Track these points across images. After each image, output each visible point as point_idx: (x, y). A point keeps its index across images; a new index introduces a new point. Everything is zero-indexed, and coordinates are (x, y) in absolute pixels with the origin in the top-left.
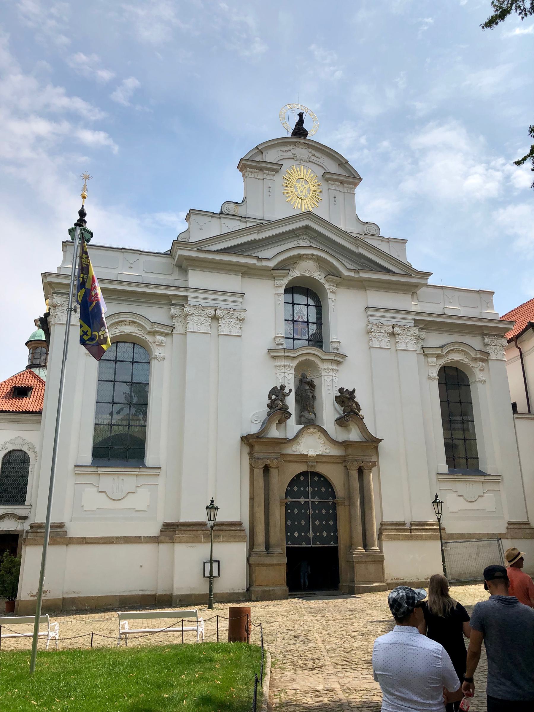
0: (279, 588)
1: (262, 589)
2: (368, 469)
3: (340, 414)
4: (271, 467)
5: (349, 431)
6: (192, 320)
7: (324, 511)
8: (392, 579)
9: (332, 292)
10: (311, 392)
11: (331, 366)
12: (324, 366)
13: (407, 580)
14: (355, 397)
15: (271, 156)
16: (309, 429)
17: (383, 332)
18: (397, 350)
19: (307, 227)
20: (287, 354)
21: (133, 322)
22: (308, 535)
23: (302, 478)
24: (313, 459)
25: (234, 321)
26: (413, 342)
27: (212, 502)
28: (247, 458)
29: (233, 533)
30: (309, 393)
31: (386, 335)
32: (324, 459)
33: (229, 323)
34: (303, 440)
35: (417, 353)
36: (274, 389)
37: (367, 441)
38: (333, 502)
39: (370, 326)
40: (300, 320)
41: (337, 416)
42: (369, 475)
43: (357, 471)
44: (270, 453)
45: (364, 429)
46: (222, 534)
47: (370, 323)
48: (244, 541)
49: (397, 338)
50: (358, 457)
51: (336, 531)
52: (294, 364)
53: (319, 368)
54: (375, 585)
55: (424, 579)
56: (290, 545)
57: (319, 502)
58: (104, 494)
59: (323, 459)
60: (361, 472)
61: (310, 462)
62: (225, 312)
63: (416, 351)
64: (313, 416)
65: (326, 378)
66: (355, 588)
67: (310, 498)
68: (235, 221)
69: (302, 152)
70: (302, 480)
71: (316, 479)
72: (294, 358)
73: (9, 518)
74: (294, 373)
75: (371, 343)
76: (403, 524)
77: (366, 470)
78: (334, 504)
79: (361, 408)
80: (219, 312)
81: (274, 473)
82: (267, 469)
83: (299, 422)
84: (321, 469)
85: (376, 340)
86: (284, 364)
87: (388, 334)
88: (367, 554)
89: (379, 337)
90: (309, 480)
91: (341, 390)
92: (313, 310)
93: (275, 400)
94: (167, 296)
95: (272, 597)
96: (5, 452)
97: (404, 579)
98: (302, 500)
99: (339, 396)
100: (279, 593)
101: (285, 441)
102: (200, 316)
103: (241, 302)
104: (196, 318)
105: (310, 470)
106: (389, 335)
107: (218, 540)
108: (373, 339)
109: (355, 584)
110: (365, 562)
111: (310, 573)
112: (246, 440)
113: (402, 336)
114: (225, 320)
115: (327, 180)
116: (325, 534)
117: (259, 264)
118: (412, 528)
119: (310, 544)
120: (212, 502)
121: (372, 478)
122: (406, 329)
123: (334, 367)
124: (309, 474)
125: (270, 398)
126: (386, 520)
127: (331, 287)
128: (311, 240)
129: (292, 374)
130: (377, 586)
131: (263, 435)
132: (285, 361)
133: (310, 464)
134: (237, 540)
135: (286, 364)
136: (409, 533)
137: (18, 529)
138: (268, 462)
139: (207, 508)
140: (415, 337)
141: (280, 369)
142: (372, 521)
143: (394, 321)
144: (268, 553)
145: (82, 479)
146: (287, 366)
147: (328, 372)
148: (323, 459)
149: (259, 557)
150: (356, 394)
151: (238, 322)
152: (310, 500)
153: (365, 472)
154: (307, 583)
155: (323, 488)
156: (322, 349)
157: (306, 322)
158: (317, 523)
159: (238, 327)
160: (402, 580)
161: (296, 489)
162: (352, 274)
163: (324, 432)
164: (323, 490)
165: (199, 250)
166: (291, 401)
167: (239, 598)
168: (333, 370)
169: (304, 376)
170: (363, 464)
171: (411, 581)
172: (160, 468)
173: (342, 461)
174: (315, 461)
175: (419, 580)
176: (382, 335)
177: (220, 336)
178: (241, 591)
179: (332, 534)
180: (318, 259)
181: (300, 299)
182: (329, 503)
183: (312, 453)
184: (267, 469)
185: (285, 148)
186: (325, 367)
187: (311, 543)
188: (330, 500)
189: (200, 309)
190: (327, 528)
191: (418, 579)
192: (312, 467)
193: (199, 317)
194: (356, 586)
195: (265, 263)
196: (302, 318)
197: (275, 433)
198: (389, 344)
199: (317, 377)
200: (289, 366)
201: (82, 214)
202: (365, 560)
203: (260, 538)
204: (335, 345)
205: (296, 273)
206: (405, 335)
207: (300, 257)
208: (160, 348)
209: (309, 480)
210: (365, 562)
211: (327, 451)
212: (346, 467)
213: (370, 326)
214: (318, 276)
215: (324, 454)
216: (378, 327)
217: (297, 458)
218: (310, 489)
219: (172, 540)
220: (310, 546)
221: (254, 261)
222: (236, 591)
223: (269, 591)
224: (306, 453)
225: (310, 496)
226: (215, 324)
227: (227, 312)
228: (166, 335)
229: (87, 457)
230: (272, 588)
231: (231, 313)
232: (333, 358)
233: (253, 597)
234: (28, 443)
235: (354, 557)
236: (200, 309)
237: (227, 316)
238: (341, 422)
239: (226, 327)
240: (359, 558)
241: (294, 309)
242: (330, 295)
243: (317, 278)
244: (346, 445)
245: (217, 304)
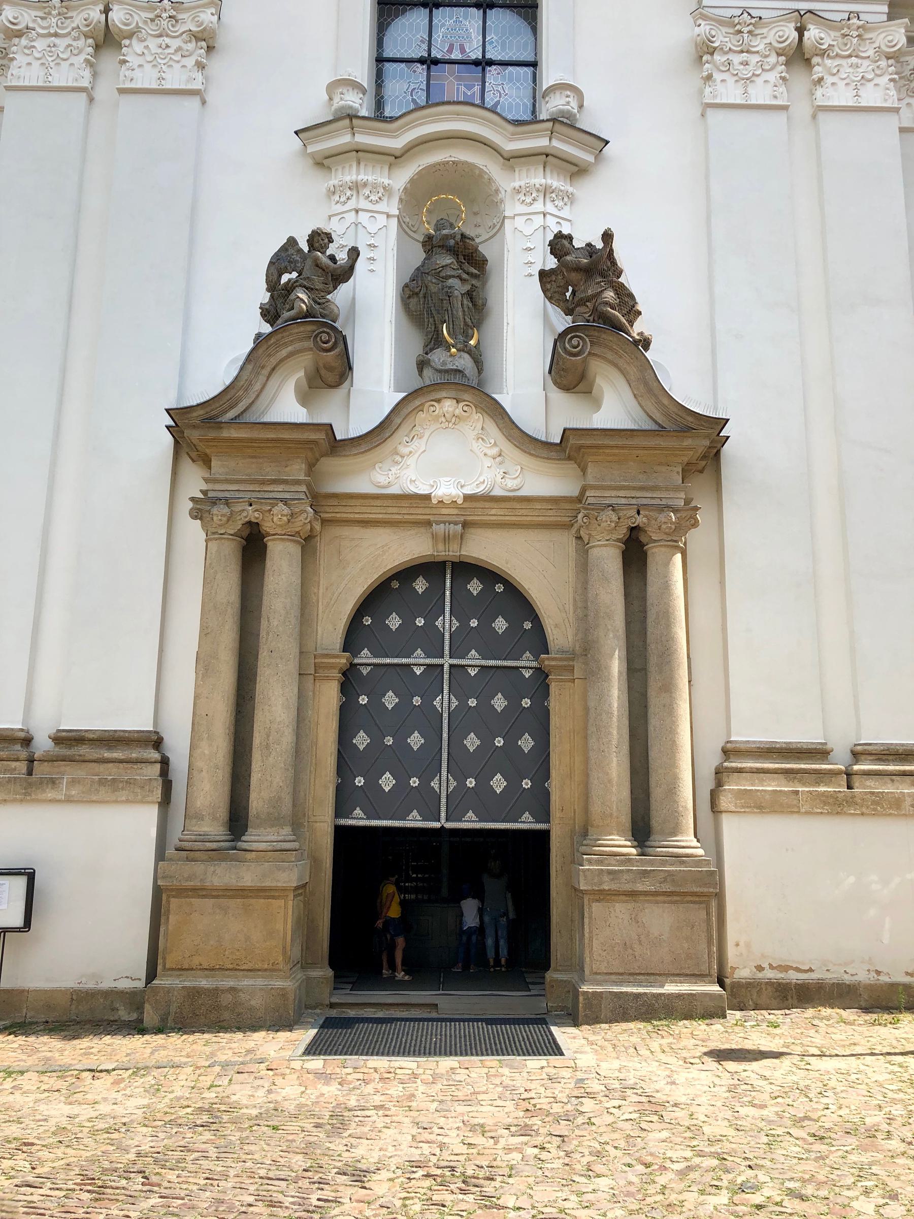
0: (260, 982)
1: (187, 984)
2: (665, 537)
4: (269, 534)
5: (597, 404)
6: (26, 51)
7: (499, 703)
8: (760, 968)
10: (460, 277)
11: (537, 178)
12: (514, 181)
13: (828, 976)
16: (438, 401)
17: (761, 47)
20: (363, 139)
22: (434, 784)
23: (420, 585)
24: (455, 512)
25: (175, 43)
26: (886, 79)
29: (110, 772)
30: (450, 281)
31: (773, 59)
32: (495, 513)
33: (160, 51)
34: (418, 445)
35: (902, 130)
36: (287, 250)
37: (660, 431)
38: (538, 670)
39: (705, 28)
40: (456, 55)
42: (668, 562)
43: (619, 547)
44: (263, 482)
45: (646, 384)
46: (70, 772)
47: (705, 17)
48: (150, 799)
49: (816, 69)
50: (622, 493)
51: (543, 771)
52: (401, 178)
53: (497, 191)
54: (671, 988)
55: (907, 973)
56: (358, 819)
57: (482, 667)
59: (493, 512)
61: (438, 523)
62: (144, 15)
63: (897, 110)
64: (465, 362)
65: (519, 222)
66: (581, 998)
67: (447, 652)
70: (420, 591)
74: (397, 212)
75: (708, 90)
76: (820, 753)
77: (655, 541)
78: (542, 675)
79: (639, 307)
85: (731, 80)
86: (354, 177)
87: (779, 55)
88: (643, 863)
89: (742, 67)
90: (448, 593)
93: (290, 288)
95: (226, 1015)
97: (811, 970)
98: (419, 660)
99: (552, 271)
100: (253, 1003)
102: (56, 35)
104: (40, 44)
105: (452, 552)
106: (782, 59)
107: (50, 794)
108: (717, 76)
109: (583, 980)
110: (632, 895)
111: (512, 915)
113: (838, 61)
114: (145, 44)
116: (498, 783)
118: (856, 767)
119: (439, 821)
122: (855, 33)
123: (549, 181)
124: (449, 572)
125: (272, 285)
126: (742, 735)
129: (388, 216)
130: (679, 996)
131: (231, 414)
132: (362, 171)
133: (440, 529)
134: (123, 795)
135: (362, 177)
136: (840, 786)
138: (251, 514)
140: (891, 62)
141: (343, 199)
142: (671, 731)
144: (235, 848)
146: (365, 185)
147: (529, 200)
148: (493, 512)
149: (188, 859)
151: (191, 46)
152: (447, 662)
153: (655, 554)
154: (504, 952)
155: (500, 619)
157: (476, 63)
158: (472, 742)
159: (190, 62)
160: (806, 971)
163: (497, 412)
164: (500, 625)
167: (114, 1009)
168: (546, 191)
170: (640, 520)
171: (847, 979)
173: (568, 519)
174: (462, 519)
175: (884, 979)
176: (754, 59)
178: (125, 985)
179: (527, 784)
182: (523, 671)
186: (517, 184)
187: (443, 815)
188: (526, 662)
189: (53, 12)
191: (878, 973)
192: (447, 539)
193: (53, 38)
194: (584, 988)
196: (463, 50)
198: (782, 89)
199: (495, 230)
200: (375, 186)
202: (628, 887)
206: (850, 56)
209: (448, 593)
210: (632, 895)
211: (511, 484)
212: (579, 538)
213: (705, 28)
215: (497, 492)
216: (740, 32)
217: (390, 510)
218: (446, 623)
220: (436, 825)
222: (107, 984)
223: (215, 992)
224: (423, 490)
225: (447, 648)
227: (152, 16)
230: (231, 983)
231: (164, 15)
232: (542, 142)
233: (150, 1016)
235: (581, 873)
236: (53, 12)
237: (151, 29)
239: (148, 67)
240: (606, 878)
241: (435, 21)
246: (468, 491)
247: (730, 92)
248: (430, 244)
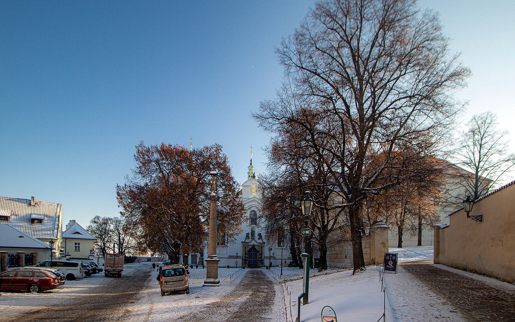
60: (261, 248)
82: (245, 247)
101: (249, 242)
184: (245, 247)
190: (255, 257)
197: (247, 241)
201: (251, 161)
203: (244, 259)
205: (252, 210)
214: (256, 210)
219: (230, 258)
244: (259, 243)
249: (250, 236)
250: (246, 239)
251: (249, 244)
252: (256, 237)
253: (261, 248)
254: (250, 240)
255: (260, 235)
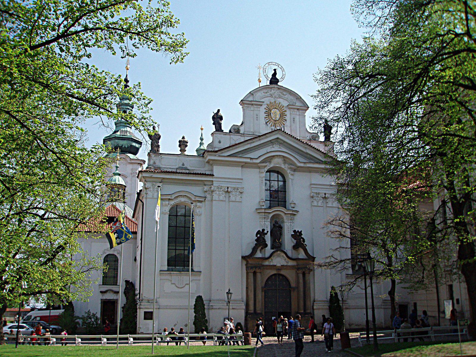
3: (293, 242)
9: (292, 175)
14: (302, 235)
15: (258, 96)
18: (327, 207)
19: (278, 138)
20: (266, 211)
21: (185, 196)
23: (273, 277)
25: (238, 193)
27: (229, 290)
28: (244, 267)
31: (321, 199)
39: (312, 195)
41: (293, 244)
52: (271, 215)
58: (174, 285)
60: (304, 274)
65: (287, 224)
68: (238, 136)
69: (275, 92)
71: (281, 277)
72: (270, 213)
73: (109, 292)
80: (229, 189)
81: (259, 275)
82: (255, 273)
83: (272, 248)
84: (283, 272)
91: (294, 231)
92: (281, 183)
94: (203, 180)
96: (105, 255)
103: (241, 183)
104: (218, 192)
112: (243, 258)
115: (289, 108)
117: (251, 161)
120: (229, 290)
121: (309, 277)
125: (257, 236)
127: (291, 172)
128: (281, 145)
137: (115, 298)
139: (227, 293)
143: (325, 192)
145: (163, 277)
150: (302, 233)
153: (307, 275)
156: (285, 207)
159: (240, 196)
161: (270, 282)
162: (302, 165)
165: (219, 156)
166: (268, 238)
169: (276, 222)
172: (200, 272)
177: (231, 203)
180: (284, 157)
181: (274, 176)
183: (279, 265)
184: (255, 273)
185: (265, 91)
195: (255, 161)
197: (259, 255)
203: (252, 308)
204: (293, 205)
207: (274, 156)
208: (199, 209)
214: (284, 167)
218: (278, 282)
221: (249, 160)
224: (275, 264)
226: (227, 194)
228: (201, 202)
229: (166, 268)
234: (117, 250)
238: (295, 247)
242: (290, 177)
243: (283, 167)
245: (229, 186)
246: (282, 264)
247: (315, 203)
248: (274, 225)
249: (268, 238)
250: (254, 250)
251: (267, 263)
252: (288, 242)
253: (304, 274)
254: (268, 251)
255: (297, 235)
